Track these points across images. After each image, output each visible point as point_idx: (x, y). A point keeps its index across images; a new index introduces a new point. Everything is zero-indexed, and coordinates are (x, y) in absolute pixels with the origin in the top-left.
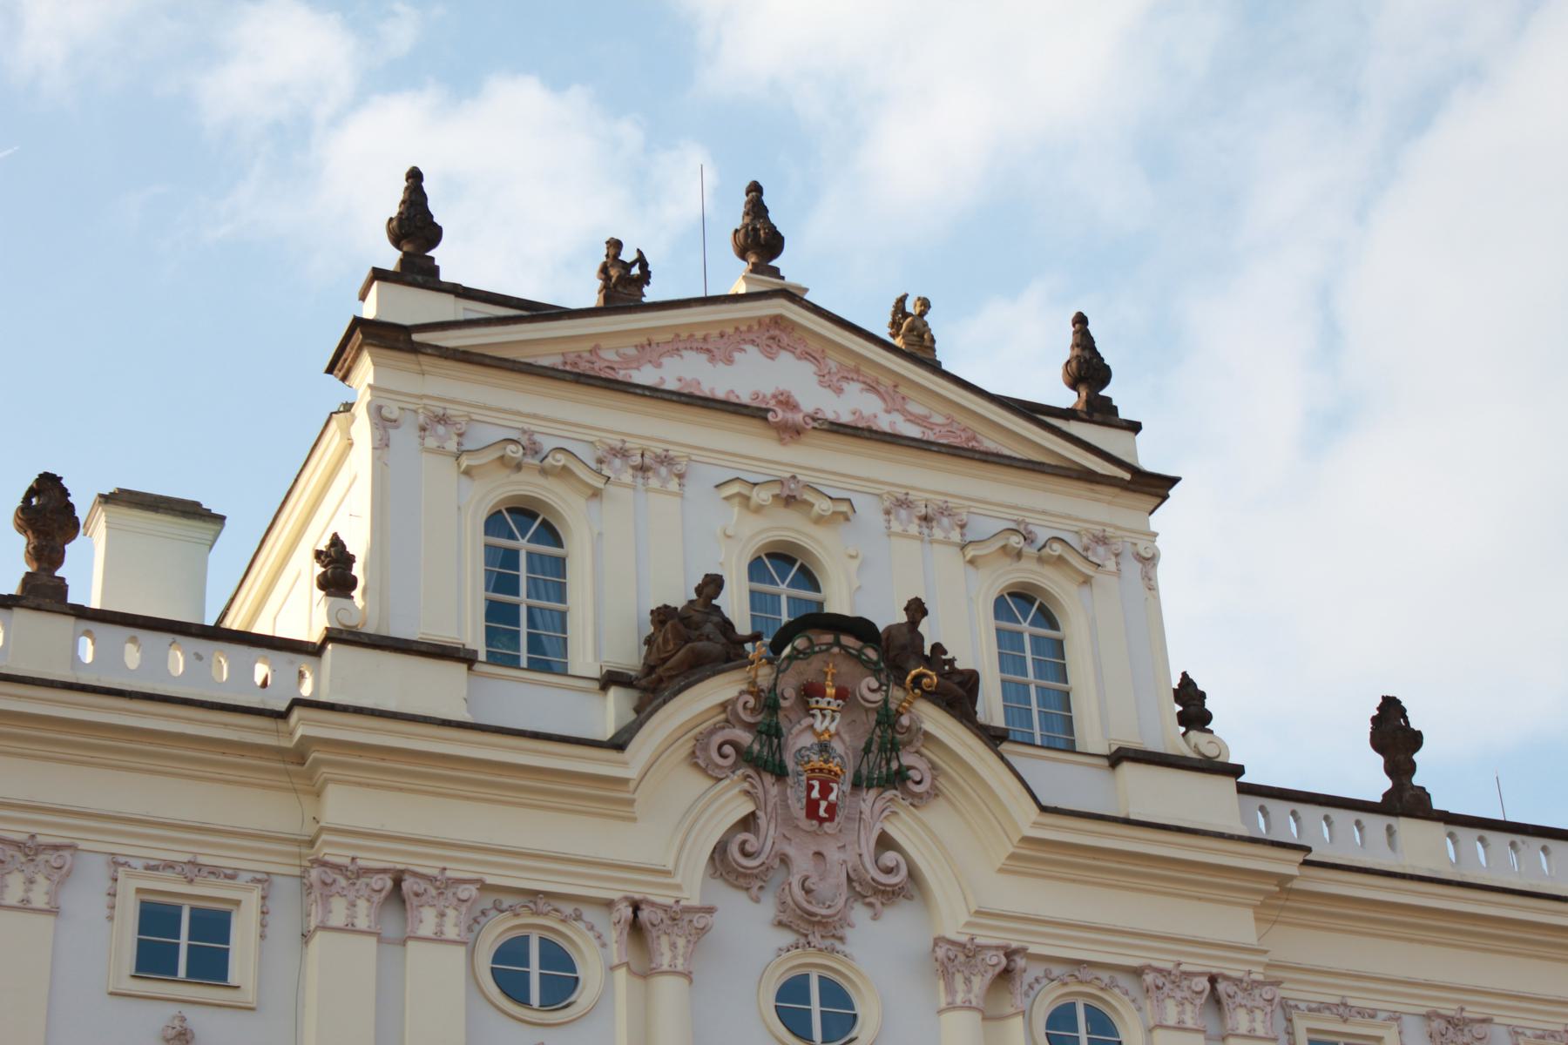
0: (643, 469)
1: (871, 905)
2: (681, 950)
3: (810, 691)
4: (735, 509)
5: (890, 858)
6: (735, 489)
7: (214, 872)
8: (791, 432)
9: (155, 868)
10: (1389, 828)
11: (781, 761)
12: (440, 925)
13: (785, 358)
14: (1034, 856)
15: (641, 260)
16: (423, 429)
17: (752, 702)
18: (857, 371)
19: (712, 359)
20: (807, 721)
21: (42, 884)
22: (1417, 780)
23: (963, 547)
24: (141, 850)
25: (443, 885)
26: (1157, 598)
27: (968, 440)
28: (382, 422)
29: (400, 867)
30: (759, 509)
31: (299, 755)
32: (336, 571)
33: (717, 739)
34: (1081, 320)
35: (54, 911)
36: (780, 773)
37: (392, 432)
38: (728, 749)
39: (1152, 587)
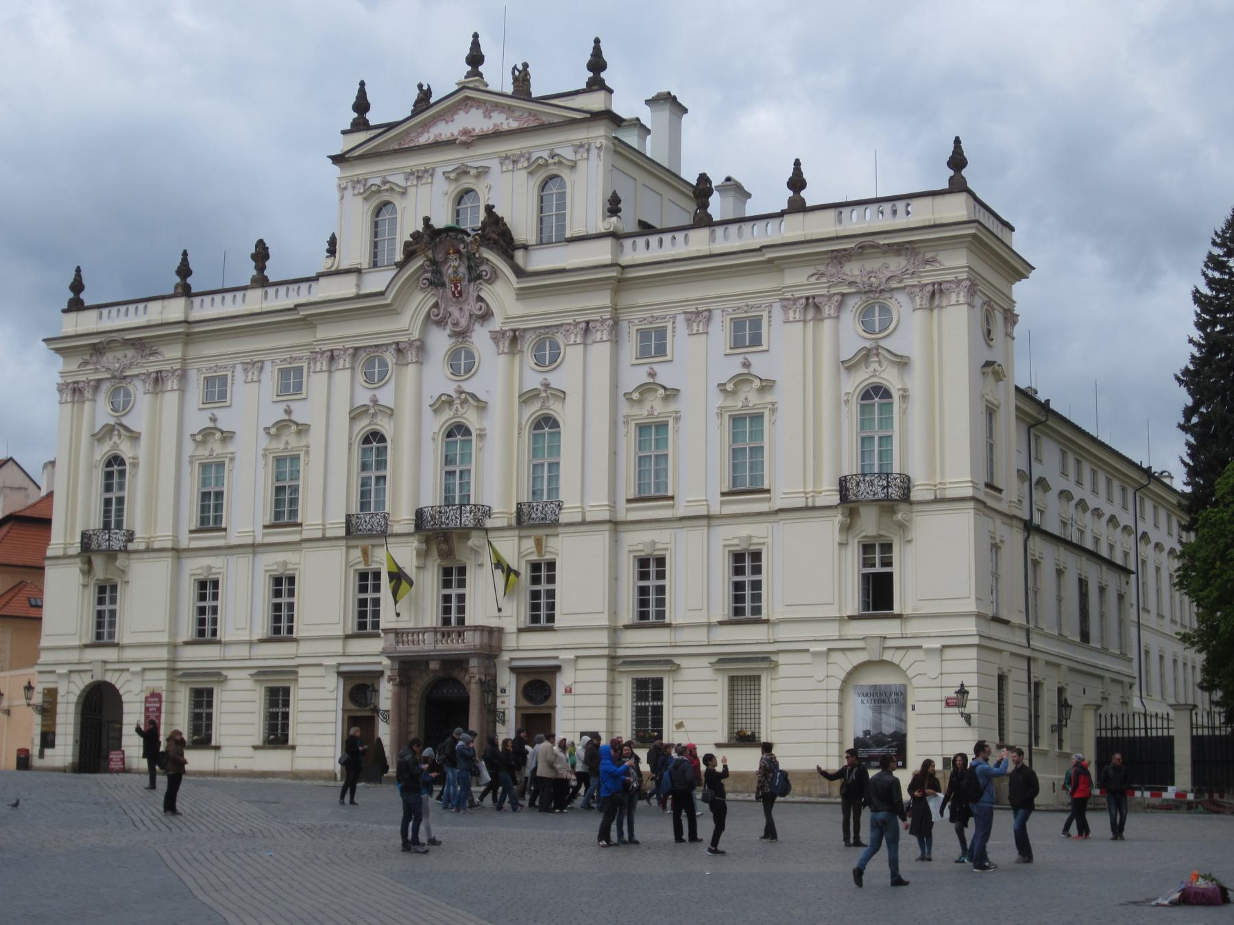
0: (418, 178)
8: (466, 145)
15: (429, 88)
18: (497, 106)
25: (346, 350)
30: (456, 180)
36: (443, 285)
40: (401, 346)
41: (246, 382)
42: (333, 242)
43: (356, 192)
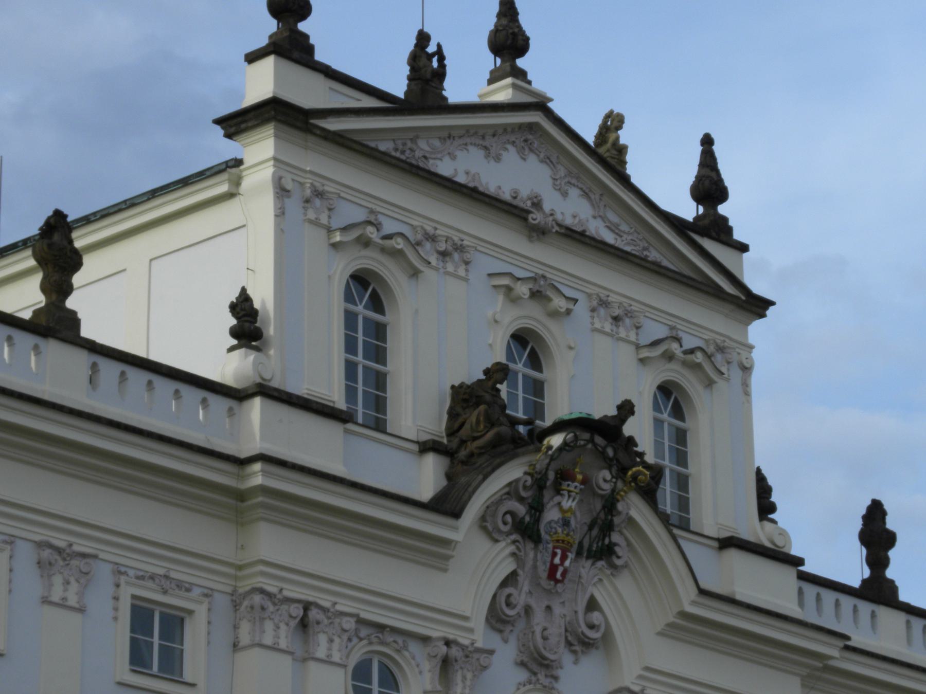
0: (444, 254)
1: (574, 652)
2: (468, 683)
3: (564, 476)
4: (501, 298)
5: (595, 617)
6: (505, 281)
7: (180, 585)
8: (538, 232)
9: (142, 578)
10: (873, 613)
11: (538, 530)
12: (330, 649)
13: (532, 158)
14: (687, 628)
15: (440, 53)
16: (307, 201)
17: (529, 479)
19: (487, 156)
20: (557, 499)
21: (74, 587)
22: (890, 573)
23: (638, 347)
24: (135, 562)
26: (749, 402)
27: (645, 249)
28: (281, 192)
29: (311, 599)
31: (241, 496)
32: (247, 326)
33: (503, 509)
34: (707, 141)
35: (81, 610)
37: (286, 200)
38: (509, 518)
39: (747, 394)
40: (454, 652)
41: (46, 601)
42: (243, 308)
43: (311, 215)
